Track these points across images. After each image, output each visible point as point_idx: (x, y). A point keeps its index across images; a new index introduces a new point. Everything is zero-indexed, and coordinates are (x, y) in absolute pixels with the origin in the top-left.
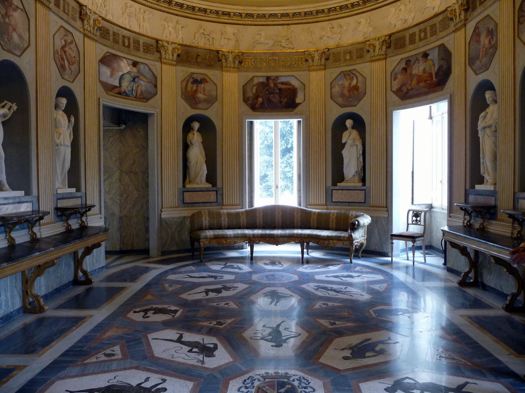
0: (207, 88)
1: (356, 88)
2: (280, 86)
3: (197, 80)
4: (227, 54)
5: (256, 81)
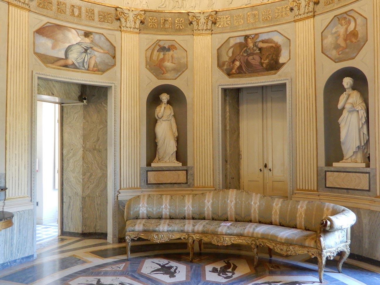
0: (175, 56)
1: (354, 34)
2: (261, 45)
3: (165, 48)
4: (198, 15)
5: (232, 42)
